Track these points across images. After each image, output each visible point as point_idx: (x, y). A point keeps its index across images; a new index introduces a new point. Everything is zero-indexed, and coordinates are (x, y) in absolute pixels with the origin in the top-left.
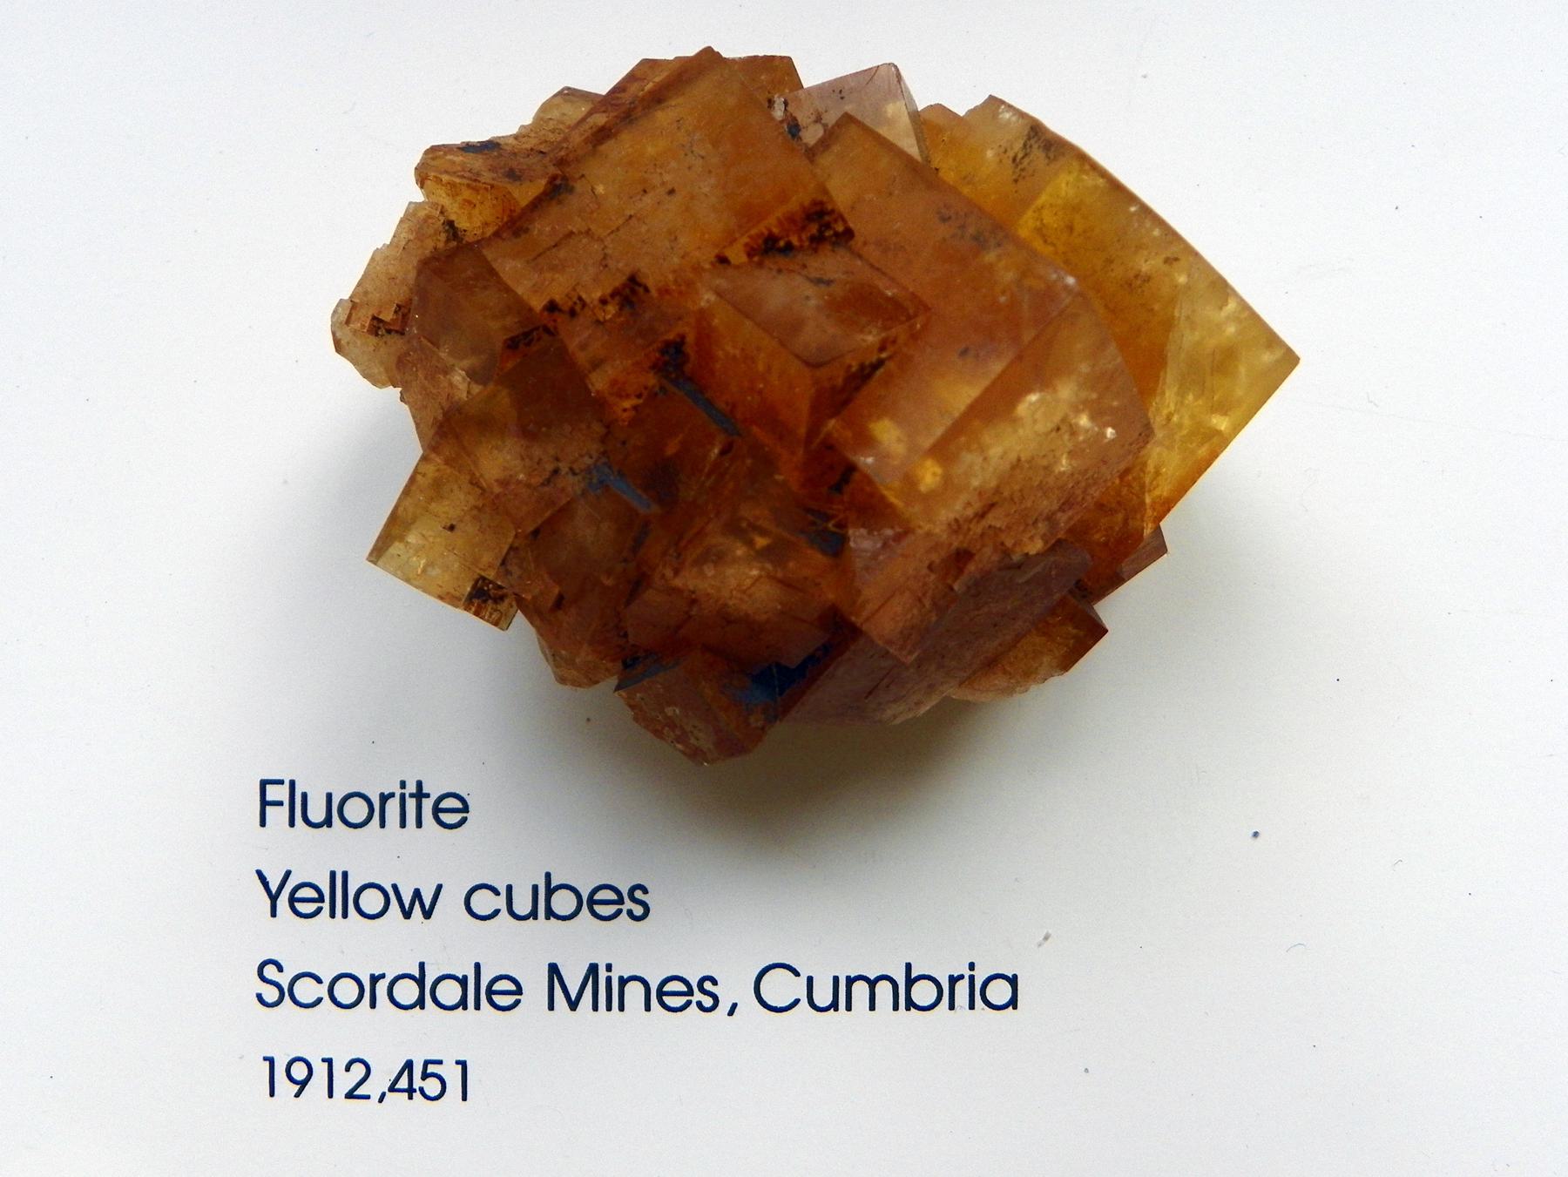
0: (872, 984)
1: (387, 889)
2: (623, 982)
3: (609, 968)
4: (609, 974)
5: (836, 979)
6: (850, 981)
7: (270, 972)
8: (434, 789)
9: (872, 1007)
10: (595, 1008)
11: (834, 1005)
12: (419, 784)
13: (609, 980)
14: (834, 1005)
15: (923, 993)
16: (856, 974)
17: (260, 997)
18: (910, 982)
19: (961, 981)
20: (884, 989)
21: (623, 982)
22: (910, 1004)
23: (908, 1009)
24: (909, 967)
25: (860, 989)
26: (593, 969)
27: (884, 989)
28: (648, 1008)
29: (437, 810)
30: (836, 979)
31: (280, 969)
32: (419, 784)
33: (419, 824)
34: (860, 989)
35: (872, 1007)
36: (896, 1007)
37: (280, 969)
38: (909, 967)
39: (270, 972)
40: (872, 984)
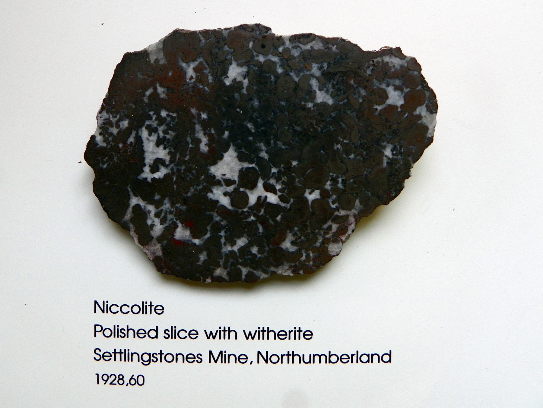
0: (320, 356)
4: (225, 353)
6: (314, 356)
7: (97, 351)
8: (155, 304)
9: (320, 362)
12: (151, 302)
14: (310, 362)
15: (333, 359)
17: (95, 358)
18: (330, 356)
20: (323, 358)
22: (330, 362)
23: (329, 363)
24: (330, 352)
25: (317, 358)
27: (323, 358)
29: (155, 310)
31: (100, 351)
32: (151, 302)
33: (151, 313)
34: (317, 358)
37: (100, 351)
38: (330, 352)
39: (97, 351)
40: (320, 356)
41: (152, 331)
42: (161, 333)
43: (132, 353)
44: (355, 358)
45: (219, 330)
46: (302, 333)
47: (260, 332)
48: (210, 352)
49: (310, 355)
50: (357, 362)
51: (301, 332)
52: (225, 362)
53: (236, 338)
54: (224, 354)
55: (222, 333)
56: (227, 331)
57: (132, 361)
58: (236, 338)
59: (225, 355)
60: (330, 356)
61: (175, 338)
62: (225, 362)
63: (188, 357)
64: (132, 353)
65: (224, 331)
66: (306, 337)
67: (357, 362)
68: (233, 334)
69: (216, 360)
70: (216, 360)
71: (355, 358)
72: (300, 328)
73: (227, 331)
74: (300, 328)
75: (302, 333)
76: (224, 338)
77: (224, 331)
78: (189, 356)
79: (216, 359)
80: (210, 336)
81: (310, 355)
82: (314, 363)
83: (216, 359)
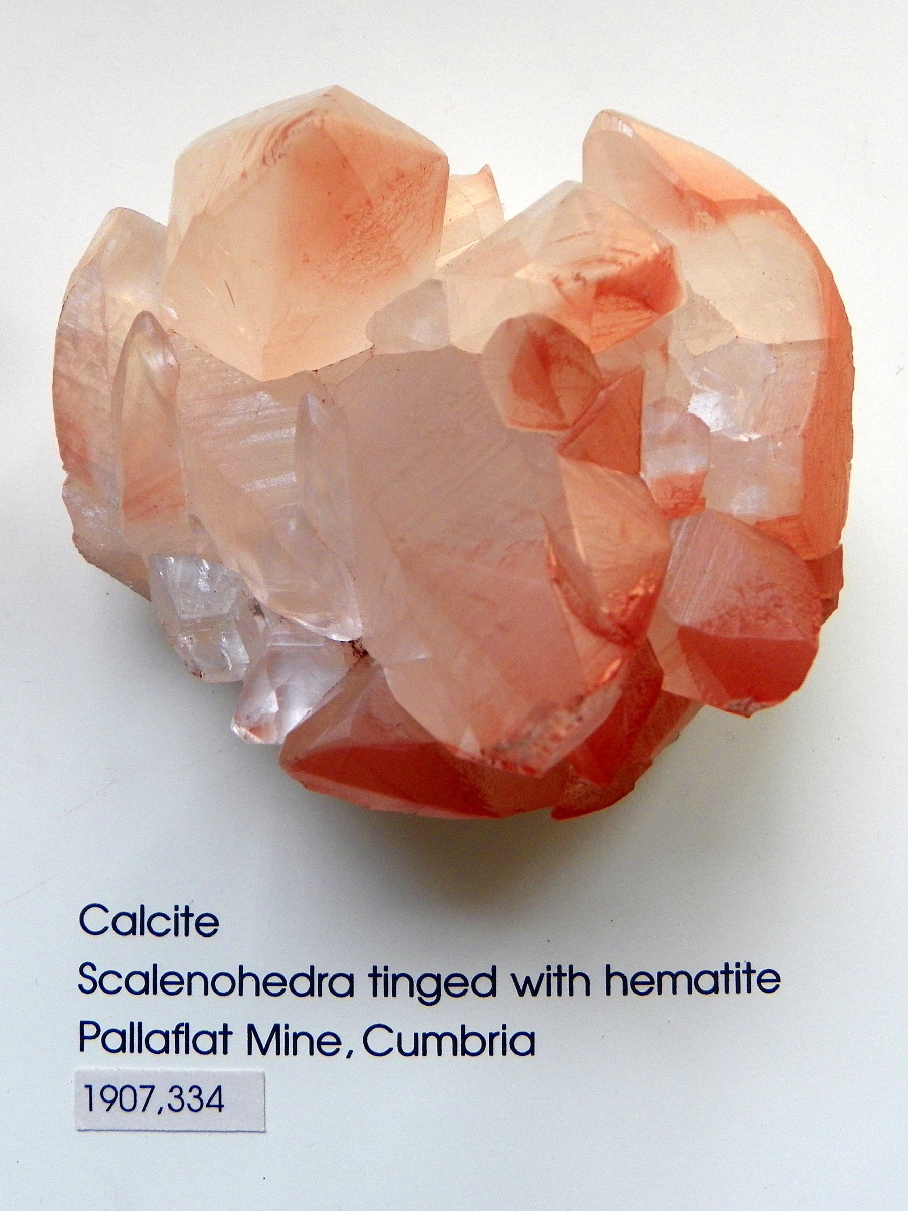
0: (440, 1038)
5: (416, 1035)
9: (440, 1053)
19: (497, 1037)
20: (447, 1042)
27: (447, 1042)
28: (312, 1053)
30: (416, 1035)
34: (432, 1042)
36: (455, 1053)
40: (440, 1038)
44: (498, 1041)
48: (251, 1028)
50: (504, 1053)
67: (504, 1053)
69: (264, 1046)
70: (264, 1046)
71: (498, 1041)
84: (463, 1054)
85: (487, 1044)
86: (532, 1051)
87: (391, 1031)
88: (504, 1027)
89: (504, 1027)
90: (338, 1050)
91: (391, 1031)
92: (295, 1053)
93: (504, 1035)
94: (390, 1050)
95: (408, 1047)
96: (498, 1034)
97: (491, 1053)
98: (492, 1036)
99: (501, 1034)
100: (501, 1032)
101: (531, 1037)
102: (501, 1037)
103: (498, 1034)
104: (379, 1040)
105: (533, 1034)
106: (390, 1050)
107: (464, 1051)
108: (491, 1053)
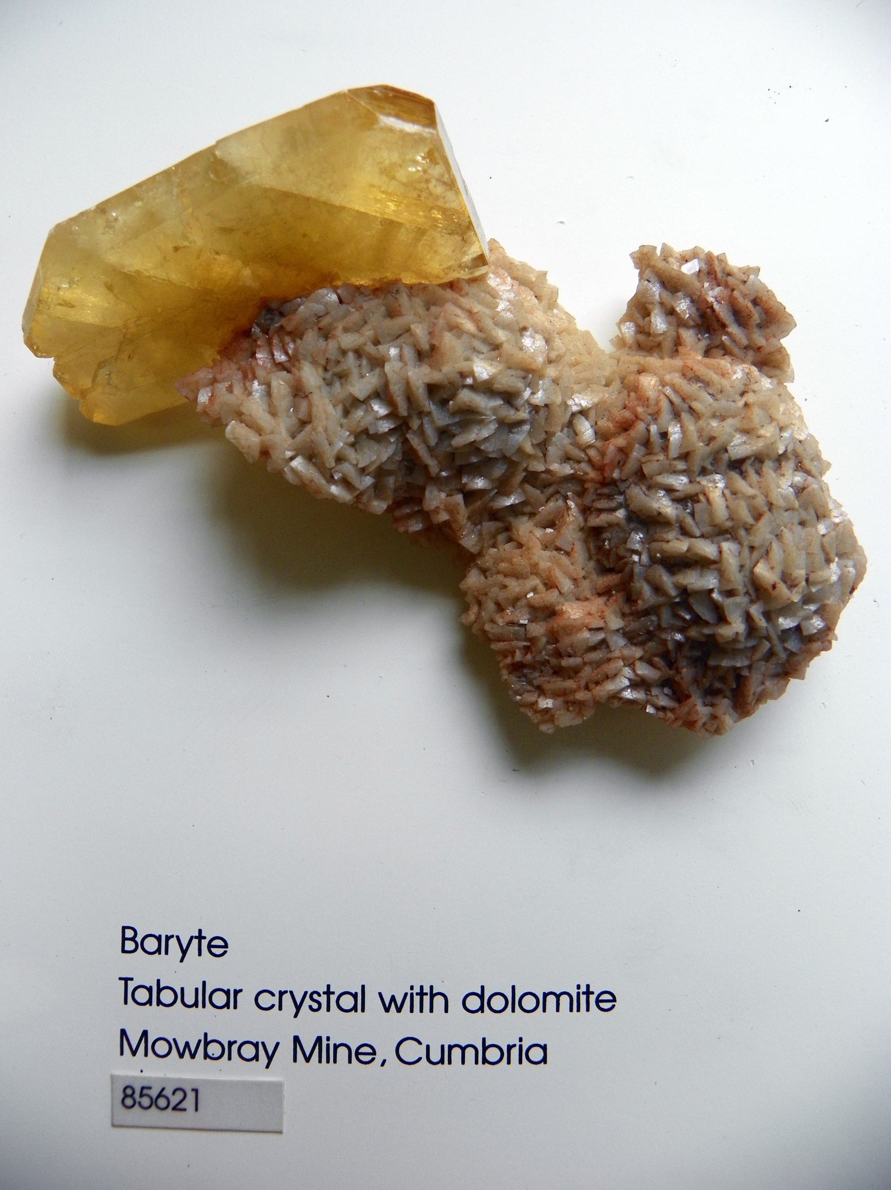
0: (463, 1049)
1: (177, 991)
2: (336, 1047)
3: (328, 1039)
6: (451, 1048)
9: (463, 1062)
10: (320, 1061)
11: (442, 1061)
13: (328, 1045)
14: (442, 1061)
16: (454, 1044)
20: (470, 1052)
21: (336, 1047)
25: (456, 1052)
26: (319, 1040)
27: (470, 1052)
34: (456, 1052)
35: (463, 1062)
36: (477, 1062)
40: (463, 1049)
41: (265, 993)
42: (372, 1001)
43: (335, 1045)
44: (515, 1052)
45: (409, 992)
46: (593, 998)
47: (581, 996)
49: (443, 1047)
50: (520, 1062)
51: (591, 996)
52: (328, 1061)
53: (446, 1011)
54: (324, 1043)
55: (417, 999)
56: (426, 994)
57: (335, 1061)
58: (446, 1011)
59: (328, 1045)
60: (485, 1048)
61: (204, 1006)
62: (328, 1061)
63: (360, 1051)
64: (335, 1045)
65: (422, 994)
66: (602, 1005)
67: (520, 1062)
68: (439, 1001)
71: (515, 1052)
72: (588, 986)
73: (426, 994)
74: (588, 986)
75: (593, 998)
76: (421, 1011)
77: (422, 994)
78: (362, 1050)
79: (308, 1054)
80: (391, 1005)
81: (443, 1047)
82: (450, 1062)
83: (308, 1054)
84: (483, 1063)
85: (506, 1054)
86: (544, 1060)
87: (420, 1043)
88: (521, 1040)
89: (521, 1040)
90: (373, 1059)
91: (420, 1043)
92: (335, 1061)
93: (521, 1047)
94: (420, 1059)
95: (435, 1056)
96: (514, 1045)
97: (509, 1062)
98: (510, 1048)
99: (517, 1047)
100: (518, 1043)
101: (544, 1048)
102: (517, 1048)
103: (514, 1045)
104: (410, 1051)
105: (545, 1045)
106: (420, 1059)
107: (485, 1061)
108: (509, 1062)
